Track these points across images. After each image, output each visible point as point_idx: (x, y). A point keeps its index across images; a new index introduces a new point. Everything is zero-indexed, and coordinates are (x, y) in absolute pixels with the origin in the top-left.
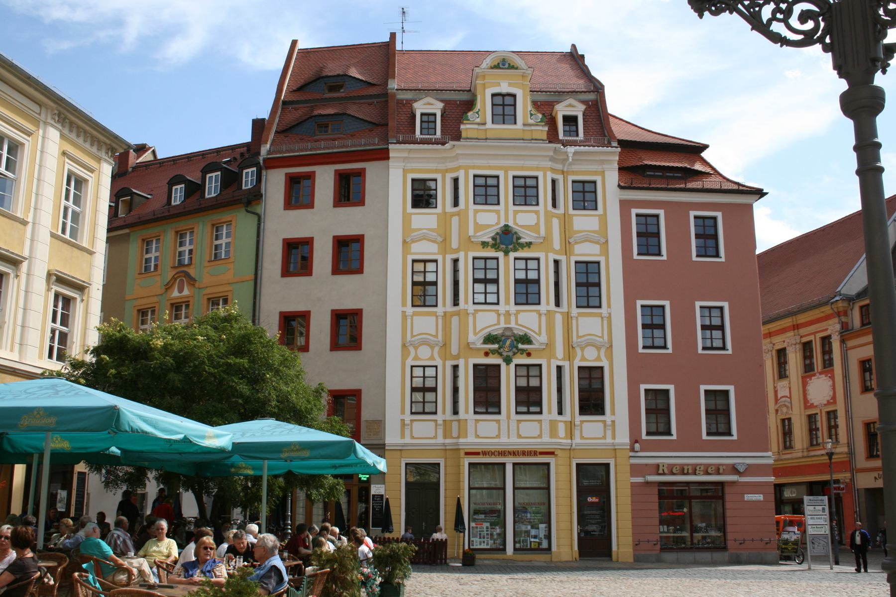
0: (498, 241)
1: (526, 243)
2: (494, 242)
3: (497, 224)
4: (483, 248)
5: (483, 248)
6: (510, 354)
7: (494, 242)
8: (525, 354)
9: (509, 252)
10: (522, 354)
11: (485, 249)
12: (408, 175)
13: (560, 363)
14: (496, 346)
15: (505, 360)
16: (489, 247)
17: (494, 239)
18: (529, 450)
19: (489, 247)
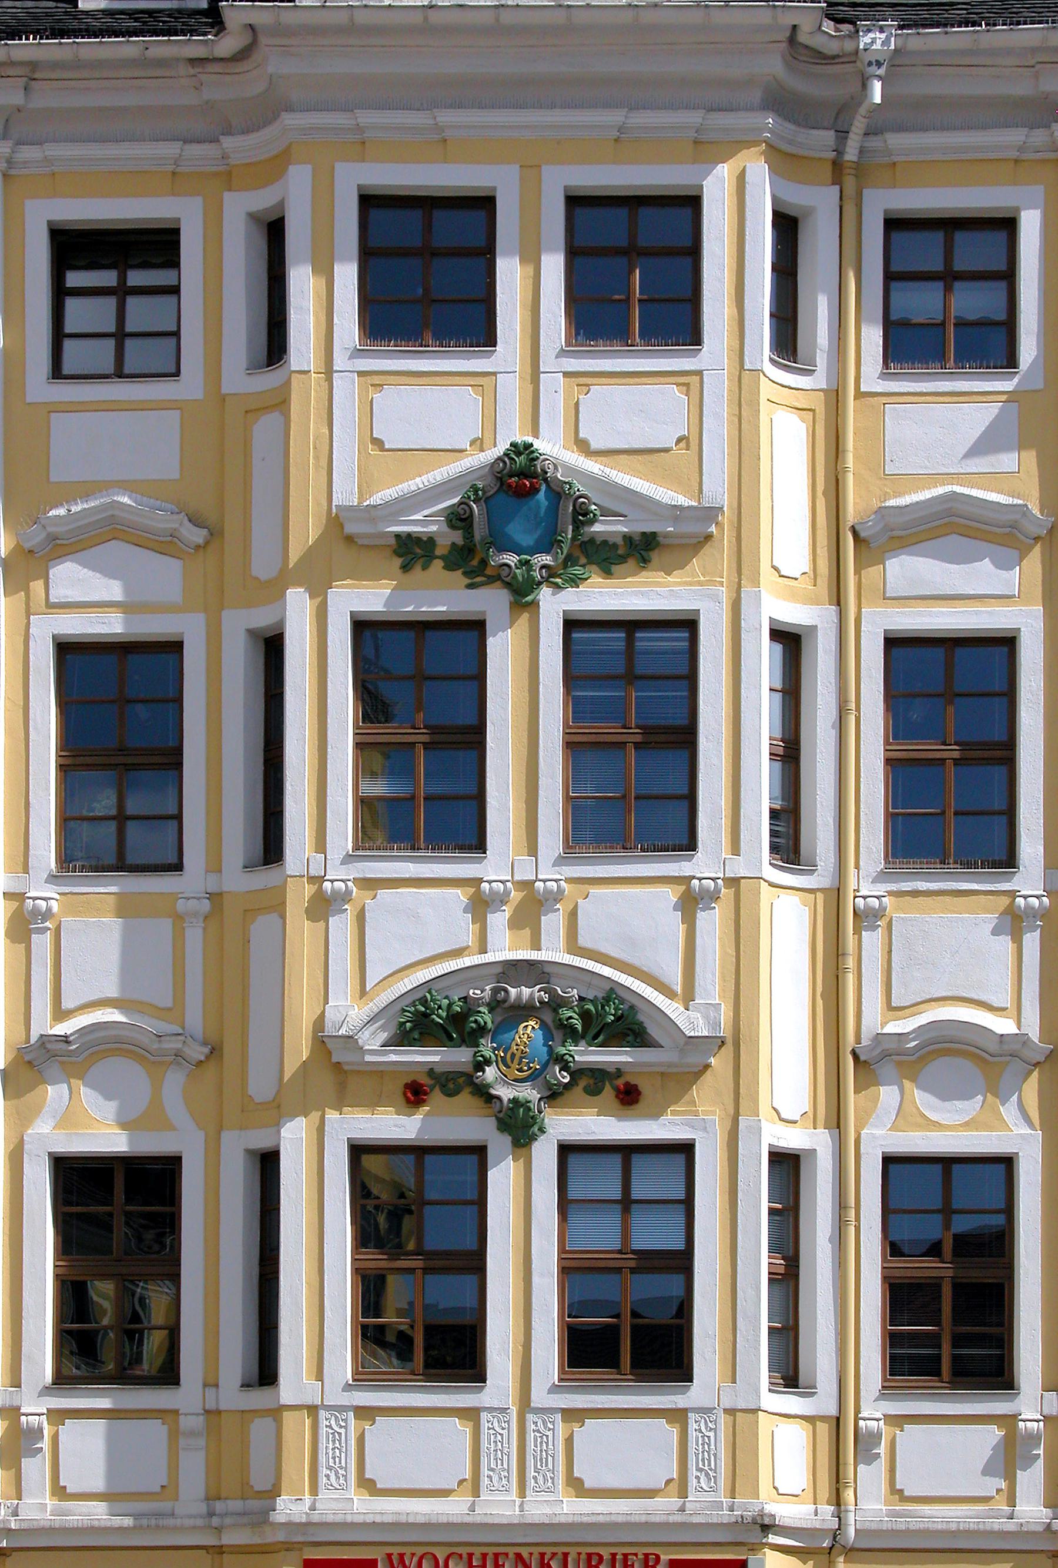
0: (480, 531)
1: (628, 538)
2: (457, 537)
3: (478, 444)
4: (406, 568)
5: (406, 568)
6: (530, 1093)
7: (457, 537)
8: (608, 1092)
9: (533, 585)
10: (594, 1091)
11: (417, 573)
12: (29, 204)
13: (793, 1139)
14: (460, 1056)
15: (504, 1125)
16: (438, 564)
17: (459, 519)
18: (620, 1551)
19: (438, 564)
